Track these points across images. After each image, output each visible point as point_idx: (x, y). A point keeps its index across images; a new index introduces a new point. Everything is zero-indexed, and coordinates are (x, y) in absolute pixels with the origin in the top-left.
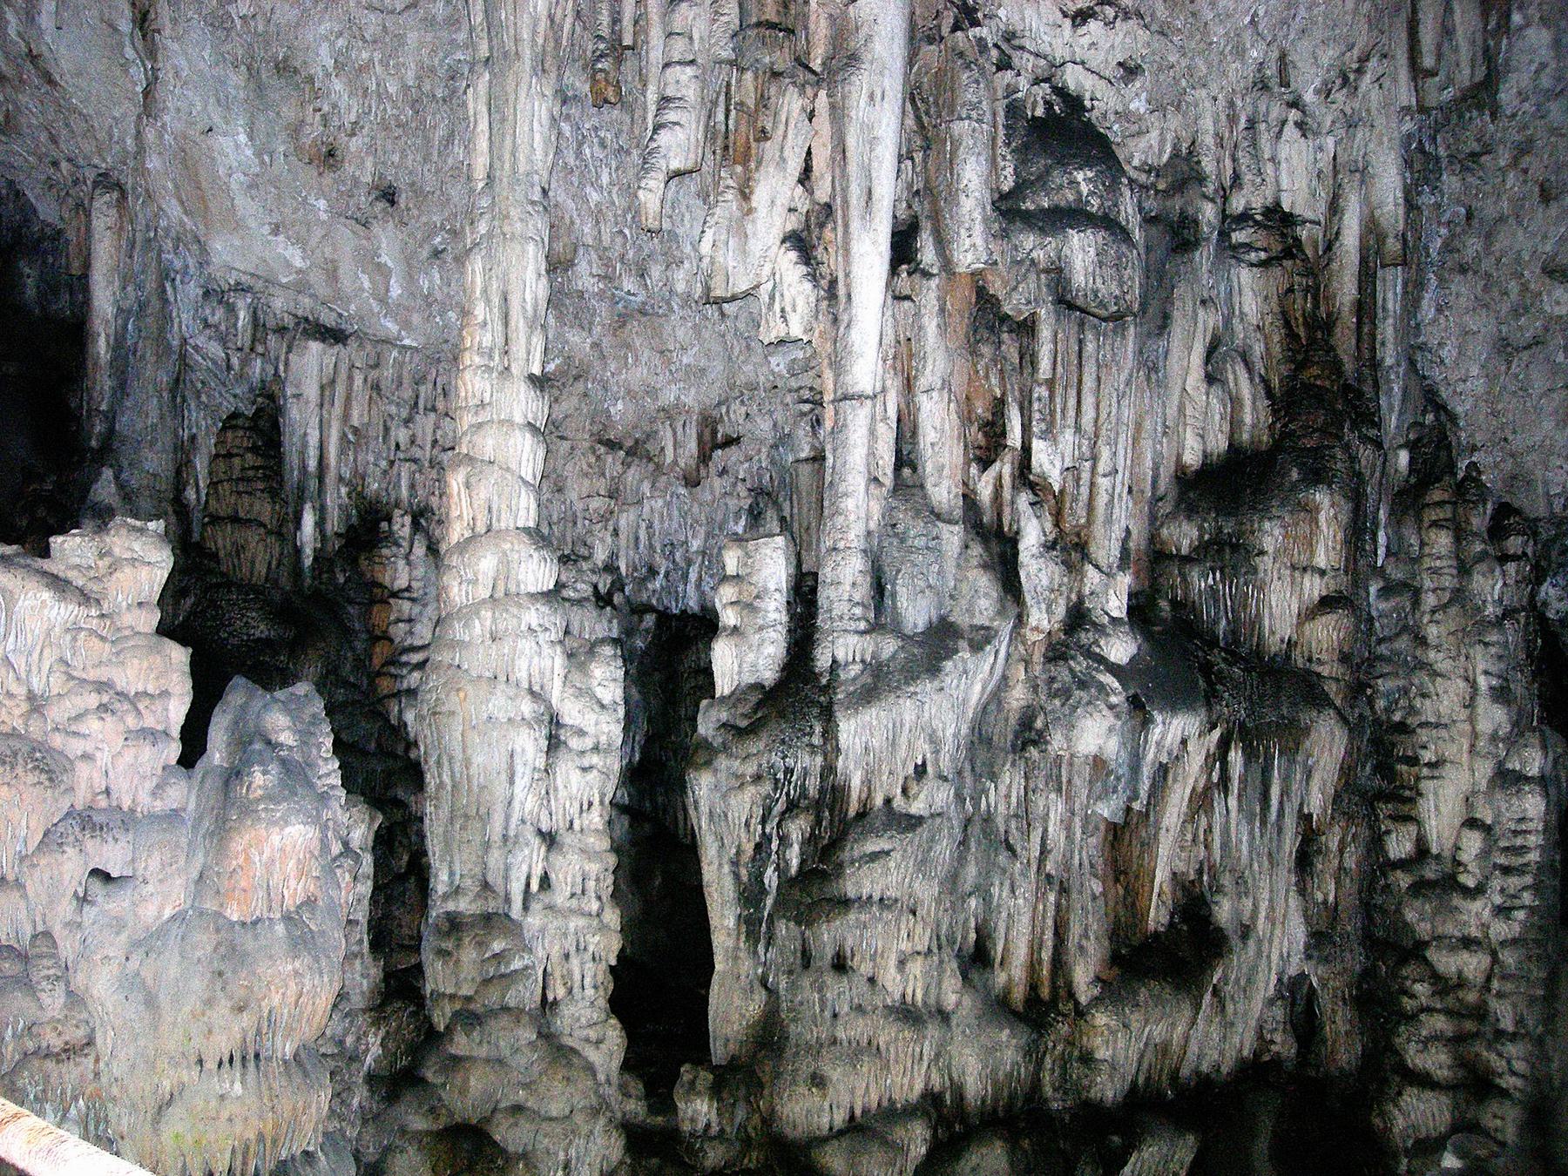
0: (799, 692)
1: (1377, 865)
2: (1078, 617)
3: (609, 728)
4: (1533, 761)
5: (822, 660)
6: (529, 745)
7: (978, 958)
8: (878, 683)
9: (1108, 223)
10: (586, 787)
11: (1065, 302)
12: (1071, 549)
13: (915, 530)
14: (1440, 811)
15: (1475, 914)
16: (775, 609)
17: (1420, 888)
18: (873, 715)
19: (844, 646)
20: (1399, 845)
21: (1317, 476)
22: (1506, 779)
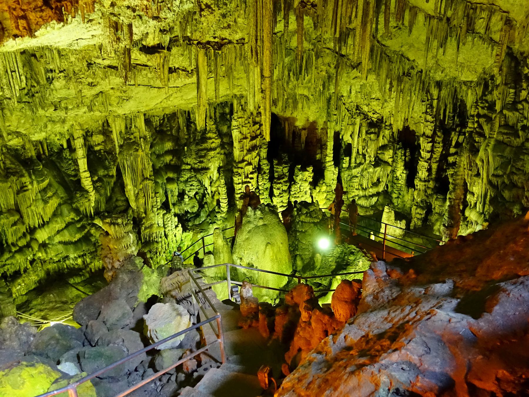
0: (349, 168)
1: (393, 177)
2: (370, 161)
3: (337, 173)
4: (405, 172)
5: (351, 165)
6: (332, 174)
7: (361, 185)
8: (355, 167)
9: (375, 133)
10: (335, 177)
11: (370, 140)
12: (370, 157)
13: (358, 156)
14: (398, 173)
15: (400, 182)
16: (348, 162)
17: (396, 179)
18: (355, 170)
19: (353, 165)
20: (395, 176)
21: (390, 149)
22: (403, 173)
